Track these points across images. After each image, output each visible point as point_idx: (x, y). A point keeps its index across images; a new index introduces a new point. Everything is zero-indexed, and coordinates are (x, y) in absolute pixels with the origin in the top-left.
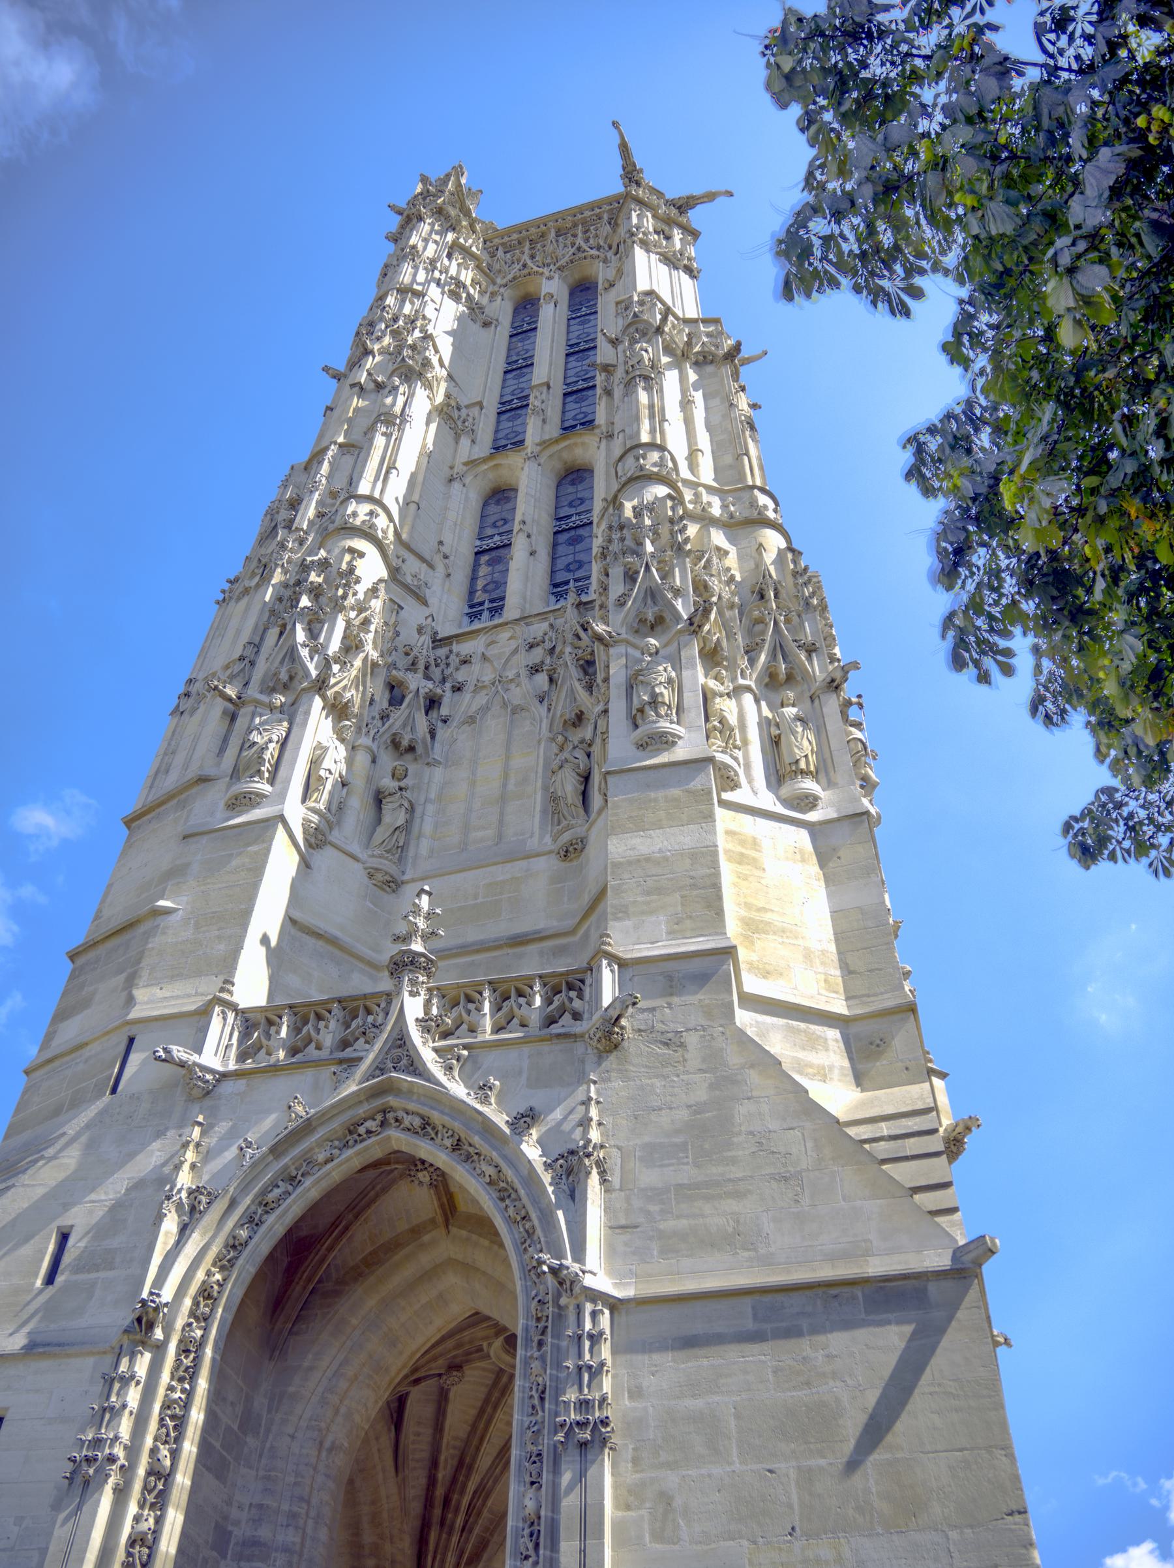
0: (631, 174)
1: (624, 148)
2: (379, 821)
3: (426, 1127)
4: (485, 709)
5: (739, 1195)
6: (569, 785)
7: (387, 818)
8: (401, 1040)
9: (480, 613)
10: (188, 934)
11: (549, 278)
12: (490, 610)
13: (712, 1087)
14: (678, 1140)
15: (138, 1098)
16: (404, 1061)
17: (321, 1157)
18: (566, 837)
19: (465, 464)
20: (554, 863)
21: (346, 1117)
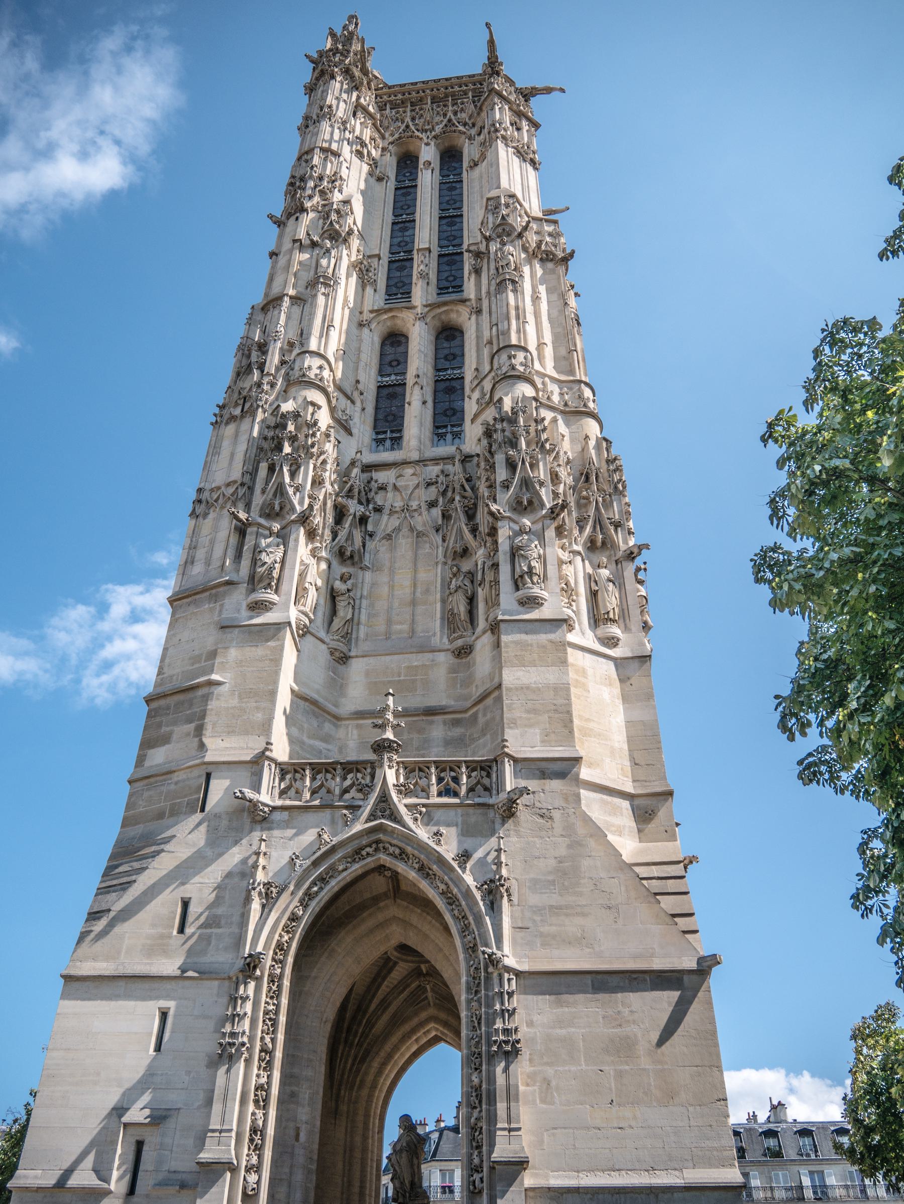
0: (493, 66)
1: (491, 43)
2: (334, 612)
3: (403, 855)
4: (398, 529)
5: (584, 915)
6: (462, 608)
7: (341, 613)
8: (384, 798)
9: (384, 440)
10: (235, 702)
11: (427, 144)
12: (392, 439)
13: (569, 847)
14: (550, 878)
15: (220, 817)
16: (388, 812)
17: (341, 868)
18: (459, 643)
19: (371, 312)
20: (450, 656)
21: (355, 844)
